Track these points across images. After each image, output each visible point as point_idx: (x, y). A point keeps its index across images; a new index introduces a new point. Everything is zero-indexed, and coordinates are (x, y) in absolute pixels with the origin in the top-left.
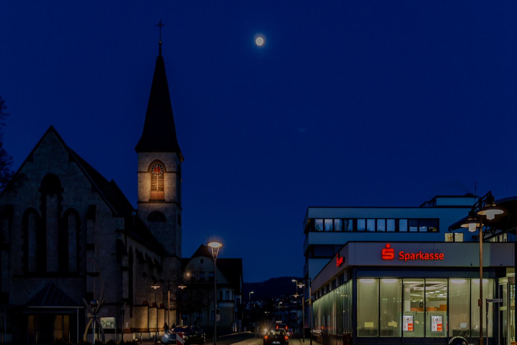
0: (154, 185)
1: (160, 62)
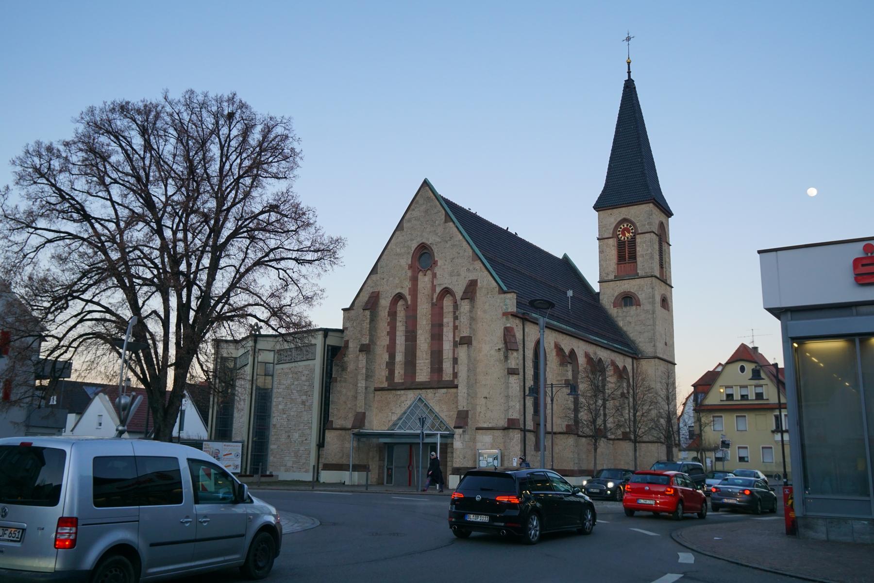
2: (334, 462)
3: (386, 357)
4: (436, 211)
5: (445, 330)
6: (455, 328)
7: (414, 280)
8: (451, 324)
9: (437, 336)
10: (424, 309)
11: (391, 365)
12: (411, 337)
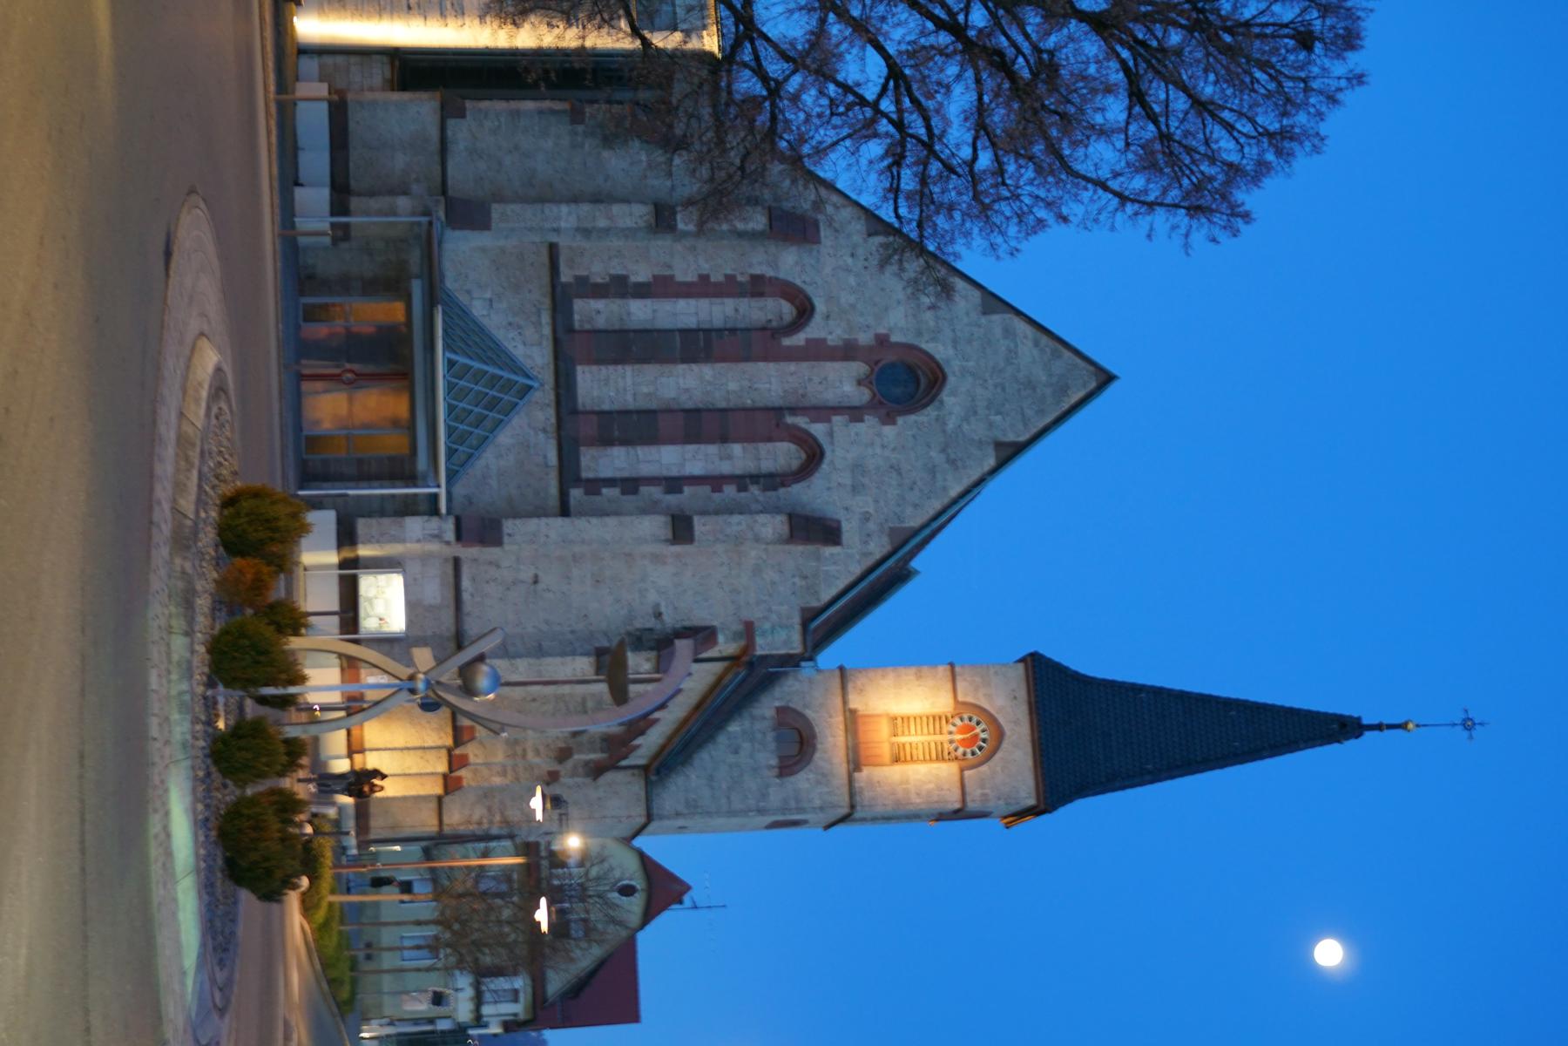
0: (909, 719)
1: (1344, 728)
2: (352, 126)
3: (641, 275)
4: (1029, 413)
5: (712, 449)
6: (715, 482)
7: (847, 352)
8: (726, 468)
9: (699, 424)
10: (767, 382)
11: (620, 287)
12: (697, 345)
